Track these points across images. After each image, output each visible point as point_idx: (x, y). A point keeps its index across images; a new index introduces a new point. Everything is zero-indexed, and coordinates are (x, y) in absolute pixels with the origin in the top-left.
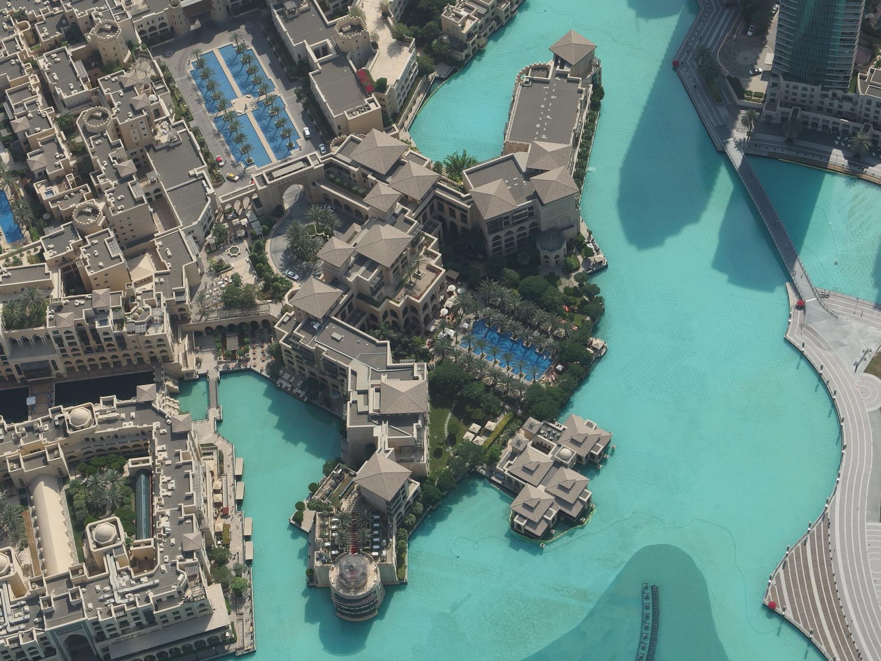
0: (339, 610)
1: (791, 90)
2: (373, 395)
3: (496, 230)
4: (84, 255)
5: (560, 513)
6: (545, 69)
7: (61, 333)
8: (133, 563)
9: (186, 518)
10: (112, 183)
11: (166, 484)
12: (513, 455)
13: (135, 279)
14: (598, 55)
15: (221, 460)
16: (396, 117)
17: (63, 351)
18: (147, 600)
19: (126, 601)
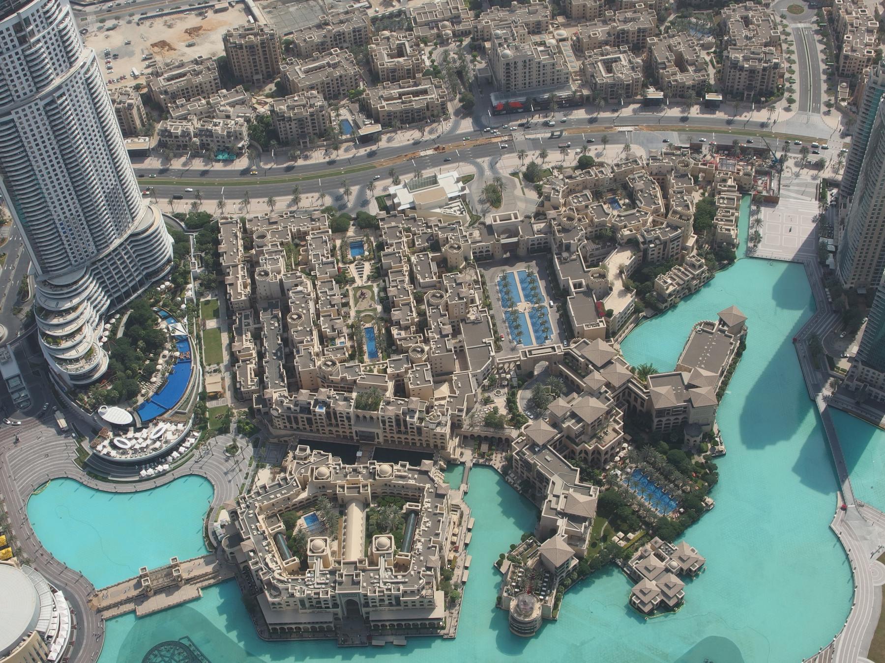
0: (511, 626)
1: (865, 372)
4: (410, 375)
5: (662, 601)
6: (713, 325)
7: (386, 418)
8: (396, 566)
10: (436, 337)
11: (426, 523)
12: (641, 557)
13: (436, 396)
14: (747, 324)
15: (461, 516)
16: (614, 334)
17: (385, 429)
18: (399, 590)
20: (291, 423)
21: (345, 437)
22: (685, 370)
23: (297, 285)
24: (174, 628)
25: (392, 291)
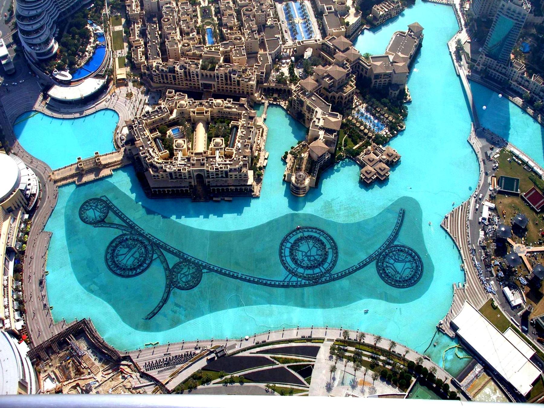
1: (487, 60)
2: (321, 120)
3: (376, 79)
5: (377, 177)
6: (404, 33)
7: (219, 74)
8: (225, 155)
9: (247, 145)
10: (249, 32)
14: (424, 32)
17: (218, 82)
19: (220, 166)
20: (163, 79)
21: (195, 87)
22: (390, 54)
23: (167, 4)
24: (97, 191)
25: (222, 7)
